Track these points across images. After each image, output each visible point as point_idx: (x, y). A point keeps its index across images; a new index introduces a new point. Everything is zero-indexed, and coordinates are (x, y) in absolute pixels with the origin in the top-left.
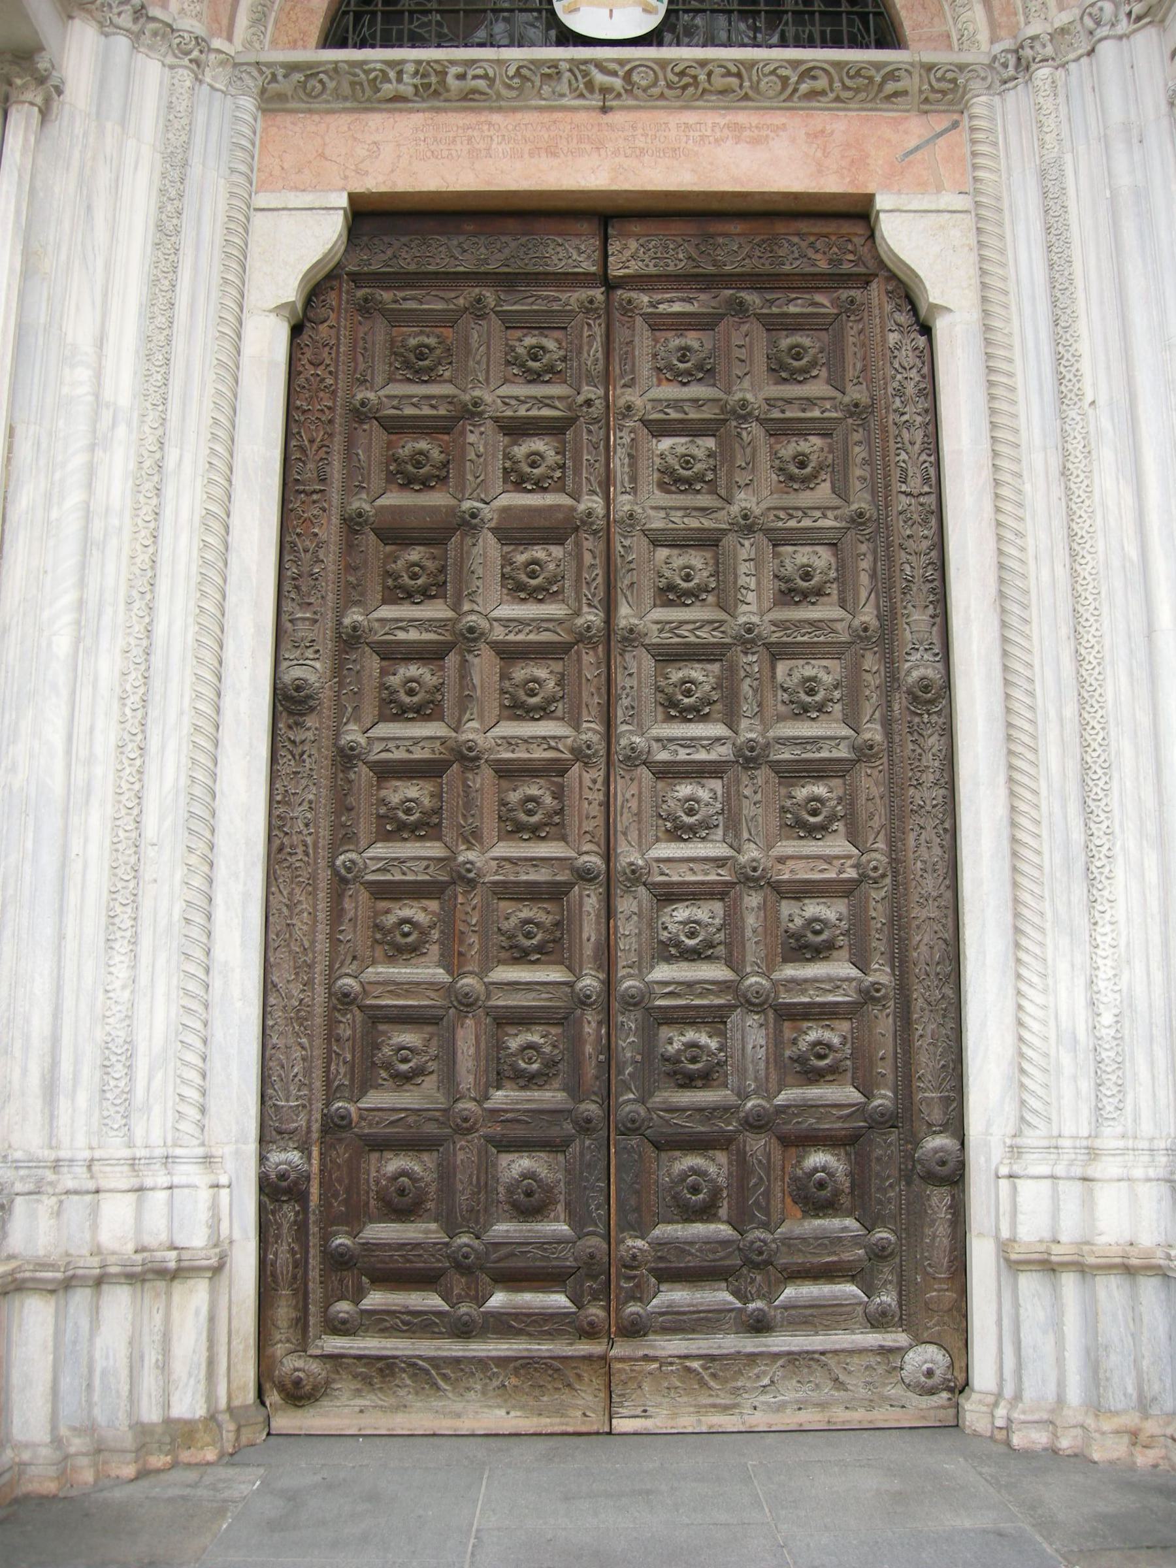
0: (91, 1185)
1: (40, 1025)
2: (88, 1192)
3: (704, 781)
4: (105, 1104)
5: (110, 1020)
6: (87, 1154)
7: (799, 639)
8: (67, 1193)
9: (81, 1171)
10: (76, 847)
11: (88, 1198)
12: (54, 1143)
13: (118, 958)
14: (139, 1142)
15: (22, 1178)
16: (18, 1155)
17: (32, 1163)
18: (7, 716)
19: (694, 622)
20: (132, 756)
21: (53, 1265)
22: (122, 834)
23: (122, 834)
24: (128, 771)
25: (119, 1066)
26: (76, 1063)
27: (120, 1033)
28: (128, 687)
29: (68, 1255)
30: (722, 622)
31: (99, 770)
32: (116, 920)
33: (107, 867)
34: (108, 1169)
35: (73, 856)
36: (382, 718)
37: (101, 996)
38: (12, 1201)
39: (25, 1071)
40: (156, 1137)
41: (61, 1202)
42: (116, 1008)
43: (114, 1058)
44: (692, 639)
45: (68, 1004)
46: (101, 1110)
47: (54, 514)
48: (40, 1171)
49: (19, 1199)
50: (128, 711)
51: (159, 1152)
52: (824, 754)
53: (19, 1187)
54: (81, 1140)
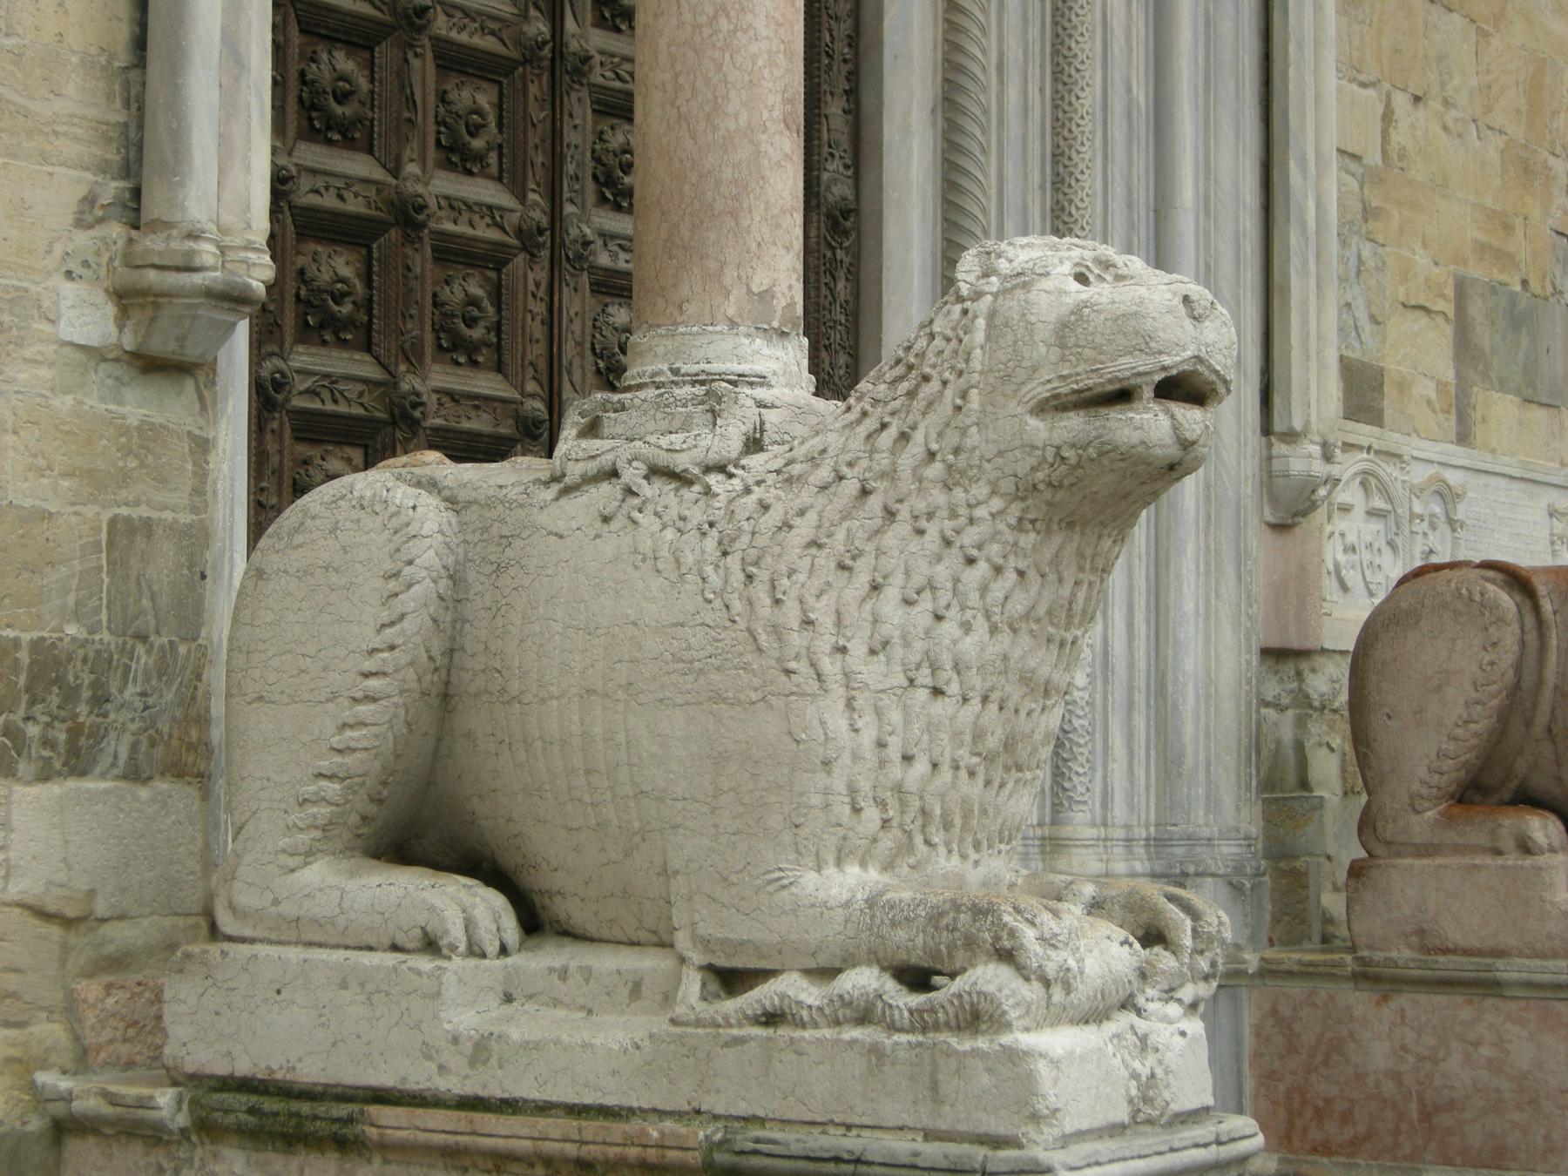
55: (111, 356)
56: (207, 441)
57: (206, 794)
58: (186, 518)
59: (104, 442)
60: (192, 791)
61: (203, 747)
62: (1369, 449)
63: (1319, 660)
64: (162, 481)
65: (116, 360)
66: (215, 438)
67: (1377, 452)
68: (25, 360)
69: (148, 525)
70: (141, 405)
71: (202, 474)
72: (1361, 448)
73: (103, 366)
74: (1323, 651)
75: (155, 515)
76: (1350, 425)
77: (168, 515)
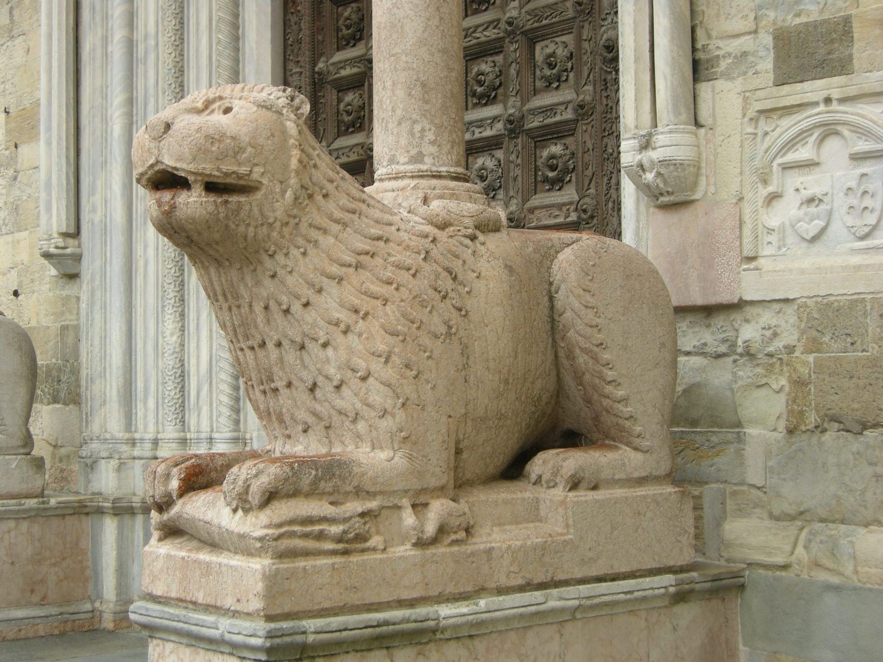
3: (494, 152)
7: (544, 22)
8: (134, 458)
9: (148, 446)
12: (133, 429)
14: (192, 429)
16: (108, 436)
17: (115, 441)
19: (483, 25)
25: (170, 383)
26: (146, 381)
30: (499, 20)
36: (339, 135)
40: (205, 426)
44: (483, 39)
46: (163, 409)
47: (110, 50)
48: (118, 446)
51: (203, 435)
52: (558, 118)
54: (151, 428)
58: (76, 323)
60: (77, 408)
61: (78, 395)
62: (828, 100)
63: (750, 311)
67: (842, 101)
69: (68, 326)
72: (816, 104)
74: (752, 303)
76: (786, 89)
77: (72, 323)
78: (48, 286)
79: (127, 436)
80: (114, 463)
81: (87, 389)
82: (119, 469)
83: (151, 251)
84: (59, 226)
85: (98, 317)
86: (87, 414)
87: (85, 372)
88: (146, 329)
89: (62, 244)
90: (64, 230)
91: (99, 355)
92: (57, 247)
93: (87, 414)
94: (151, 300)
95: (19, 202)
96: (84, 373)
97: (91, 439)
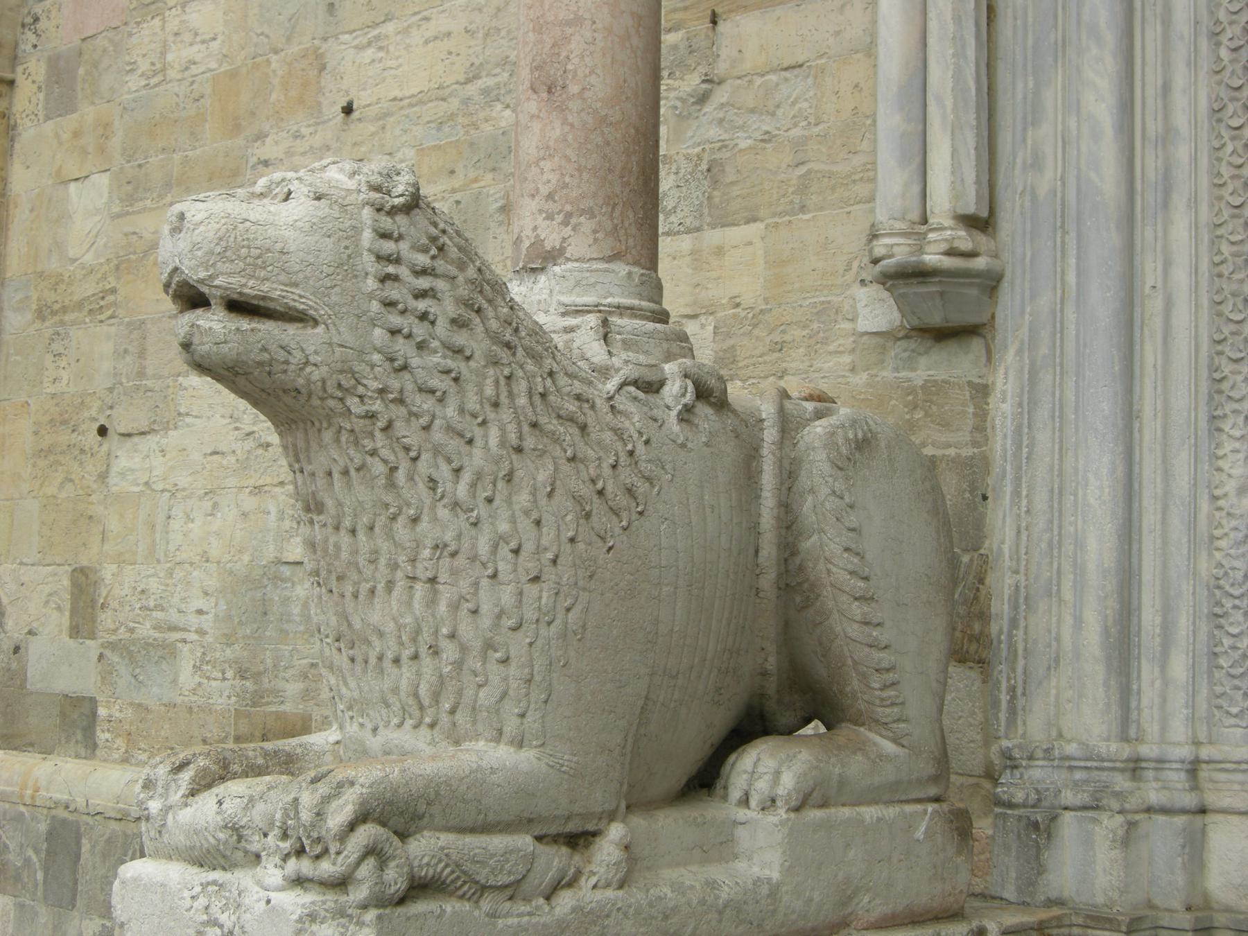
0: (1189, 800)
1: (1098, 548)
2: (1184, 811)
4: (1218, 674)
5: (1223, 543)
6: (1185, 752)
8: (1149, 810)
9: (1177, 778)
10: (1150, 272)
11: (1180, 821)
12: (1132, 733)
13: (1228, 446)
15: (1076, 784)
16: (1072, 749)
17: (1093, 761)
18: (1020, 86)
20: (1235, 123)
21: (1110, 920)
22: (1226, 249)
23: (1226, 249)
24: (1229, 148)
26: (1167, 610)
27: (1237, 564)
28: (1222, 15)
29: (1151, 906)
31: (1182, 153)
32: (1225, 386)
33: (1205, 302)
34: (1222, 776)
35: (1147, 290)
37: (1205, 506)
38: (1054, 818)
39: (1079, 622)
41: (1132, 825)
42: (1228, 524)
43: (1228, 604)
45: (1150, 518)
46: (1212, 683)
48: (1104, 775)
49: (1068, 816)
50: (1224, 53)
53: (1068, 797)
54: (1179, 730)
55: (901, 335)
56: (986, 387)
57: (986, 678)
58: (968, 452)
59: (893, 402)
60: (974, 674)
61: (981, 639)
64: (946, 425)
65: (907, 337)
66: (993, 383)
68: (830, 353)
70: (935, 366)
71: (982, 415)
73: (899, 343)
75: (939, 453)
77: (952, 452)
78: (846, 359)
79: (1126, 751)
80: (1111, 823)
81: (1014, 623)
82: (1127, 839)
83: (1181, 276)
84: (957, 196)
85: (1044, 439)
86: (1012, 690)
87: (1009, 581)
88: (1167, 475)
89: (965, 245)
90: (971, 209)
91: (1047, 536)
92: (951, 253)
93: (1012, 690)
94: (1181, 399)
95: (725, 154)
96: (1002, 584)
97: (1031, 758)
